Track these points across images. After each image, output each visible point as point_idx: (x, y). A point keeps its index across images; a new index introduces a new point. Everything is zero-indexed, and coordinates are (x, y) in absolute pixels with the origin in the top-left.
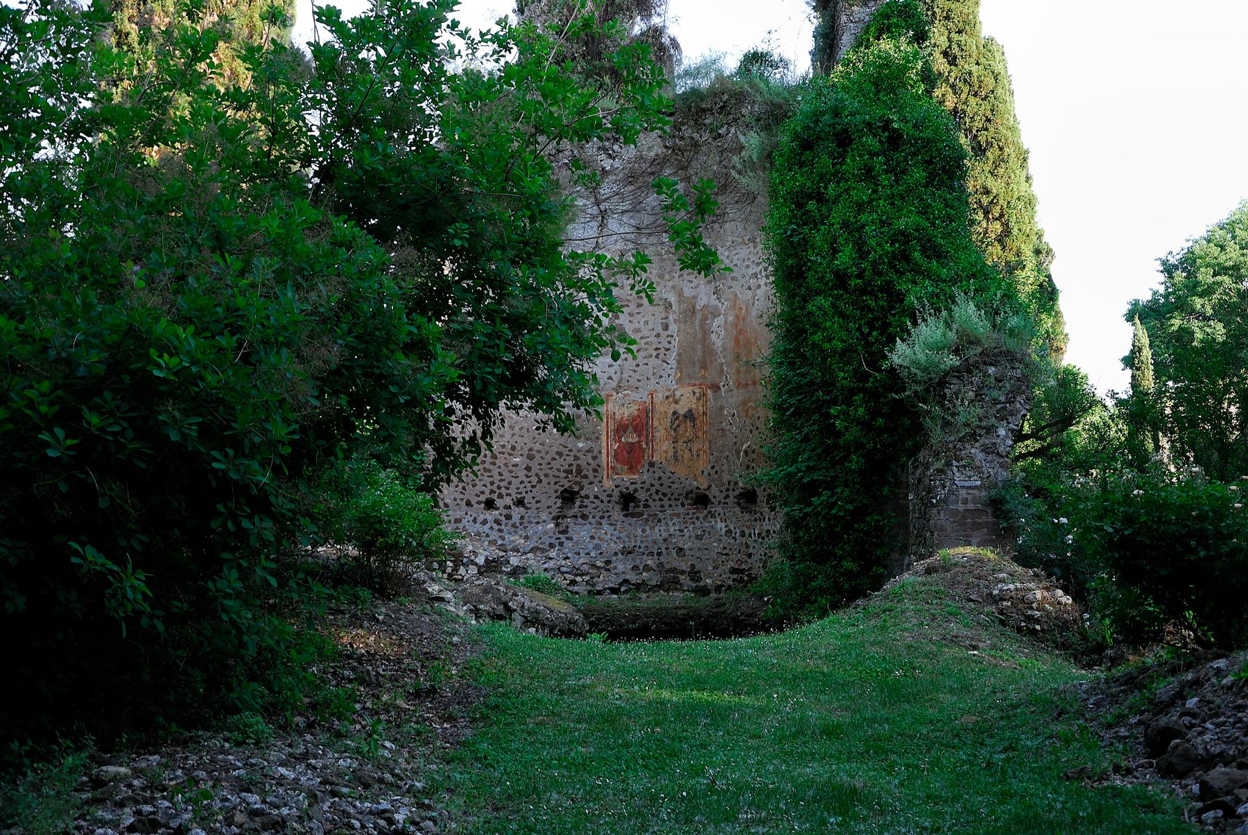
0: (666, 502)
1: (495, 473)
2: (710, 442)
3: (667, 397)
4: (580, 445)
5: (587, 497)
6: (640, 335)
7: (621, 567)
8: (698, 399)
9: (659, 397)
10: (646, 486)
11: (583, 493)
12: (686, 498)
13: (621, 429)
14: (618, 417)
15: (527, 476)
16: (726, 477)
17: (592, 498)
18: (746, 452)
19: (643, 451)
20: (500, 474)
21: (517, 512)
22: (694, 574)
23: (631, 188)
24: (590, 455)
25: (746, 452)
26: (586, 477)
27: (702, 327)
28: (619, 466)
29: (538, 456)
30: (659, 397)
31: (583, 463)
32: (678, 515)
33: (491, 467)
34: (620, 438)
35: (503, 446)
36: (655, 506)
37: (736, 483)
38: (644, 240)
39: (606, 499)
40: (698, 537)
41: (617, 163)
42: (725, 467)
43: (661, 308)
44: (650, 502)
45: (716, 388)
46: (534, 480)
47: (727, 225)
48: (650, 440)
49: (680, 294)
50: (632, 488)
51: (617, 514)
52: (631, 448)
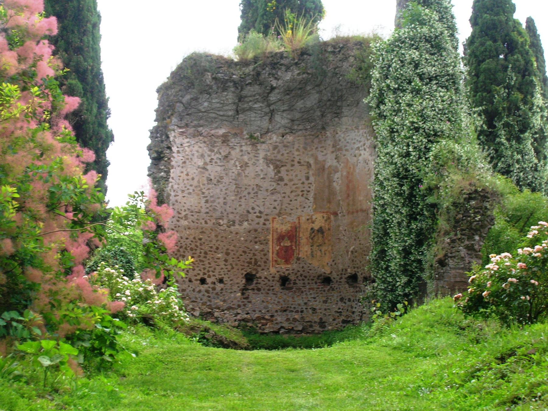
0: (306, 281)
1: (206, 262)
2: (332, 246)
3: (308, 220)
4: (257, 247)
5: (260, 278)
6: (293, 183)
7: (279, 319)
8: (326, 221)
9: (303, 219)
10: (295, 271)
11: (258, 275)
13: (281, 238)
14: (279, 231)
15: (226, 265)
16: (341, 267)
17: (263, 279)
18: (352, 252)
19: (293, 251)
20: (209, 263)
21: (219, 286)
23: (288, 97)
24: (262, 253)
25: (352, 252)
26: (260, 266)
27: (329, 178)
28: (279, 260)
29: (232, 253)
30: (303, 219)
31: (258, 258)
32: (313, 289)
33: (204, 259)
35: (211, 247)
36: (300, 283)
37: (346, 270)
38: (296, 127)
39: (271, 279)
41: (280, 82)
43: (305, 167)
44: (297, 282)
45: (335, 214)
46: (229, 267)
47: (344, 119)
48: (298, 244)
49: (316, 159)
50: (287, 273)
51: (277, 287)
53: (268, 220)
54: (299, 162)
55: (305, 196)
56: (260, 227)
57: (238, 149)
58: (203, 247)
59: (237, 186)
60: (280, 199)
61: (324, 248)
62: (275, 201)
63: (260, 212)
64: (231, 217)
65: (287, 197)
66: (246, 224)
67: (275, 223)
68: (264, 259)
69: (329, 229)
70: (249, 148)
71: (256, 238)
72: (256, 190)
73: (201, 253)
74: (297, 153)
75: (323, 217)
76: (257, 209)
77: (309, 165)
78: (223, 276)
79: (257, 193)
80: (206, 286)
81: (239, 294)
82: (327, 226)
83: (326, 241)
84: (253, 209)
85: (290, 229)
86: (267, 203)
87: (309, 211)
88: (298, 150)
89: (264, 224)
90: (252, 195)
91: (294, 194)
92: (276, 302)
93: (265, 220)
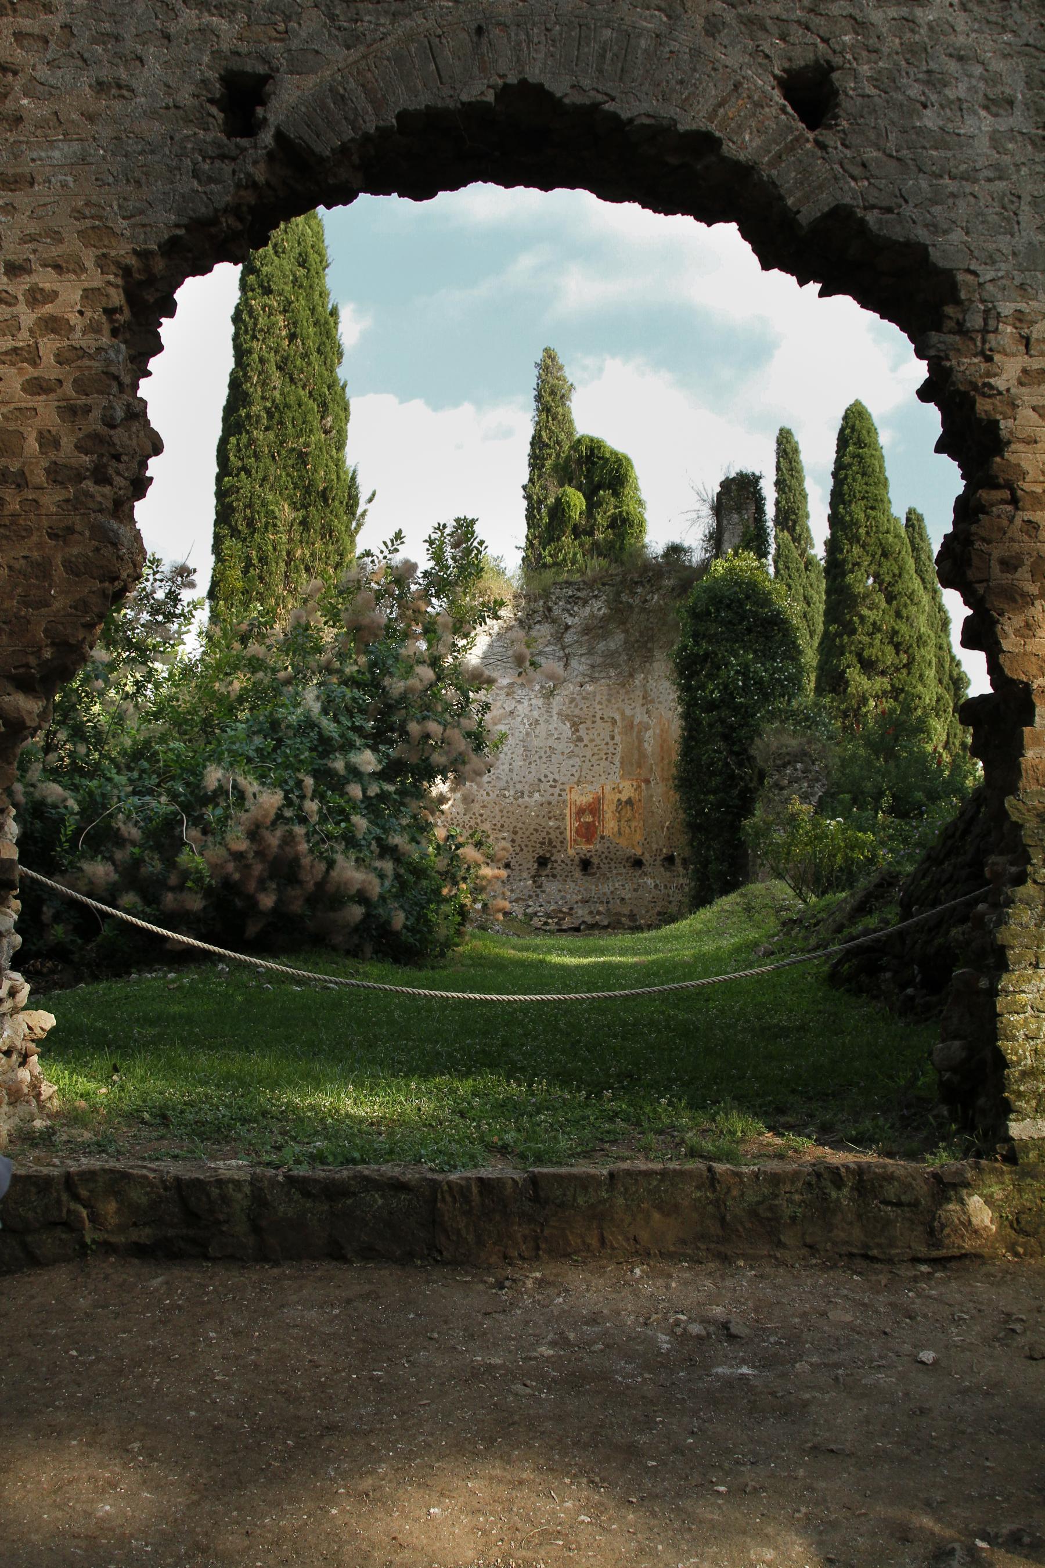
0: (613, 865)
7: (580, 912)
9: (608, 788)
13: (580, 812)
16: (654, 846)
22: (632, 917)
27: (638, 737)
30: (608, 788)
31: (553, 836)
40: (635, 890)
45: (647, 782)
46: (518, 849)
47: (655, 664)
48: (601, 820)
49: (623, 714)
51: (578, 874)
56: (554, 800)
57: (526, 703)
59: (526, 749)
61: (633, 824)
63: (555, 781)
64: (519, 787)
66: (537, 795)
68: (561, 838)
70: (540, 702)
74: (599, 707)
76: (551, 777)
77: (614, 722)
84: (546, 776)
87: (615, 778)
88: (600, 703)
90: (544, 760)
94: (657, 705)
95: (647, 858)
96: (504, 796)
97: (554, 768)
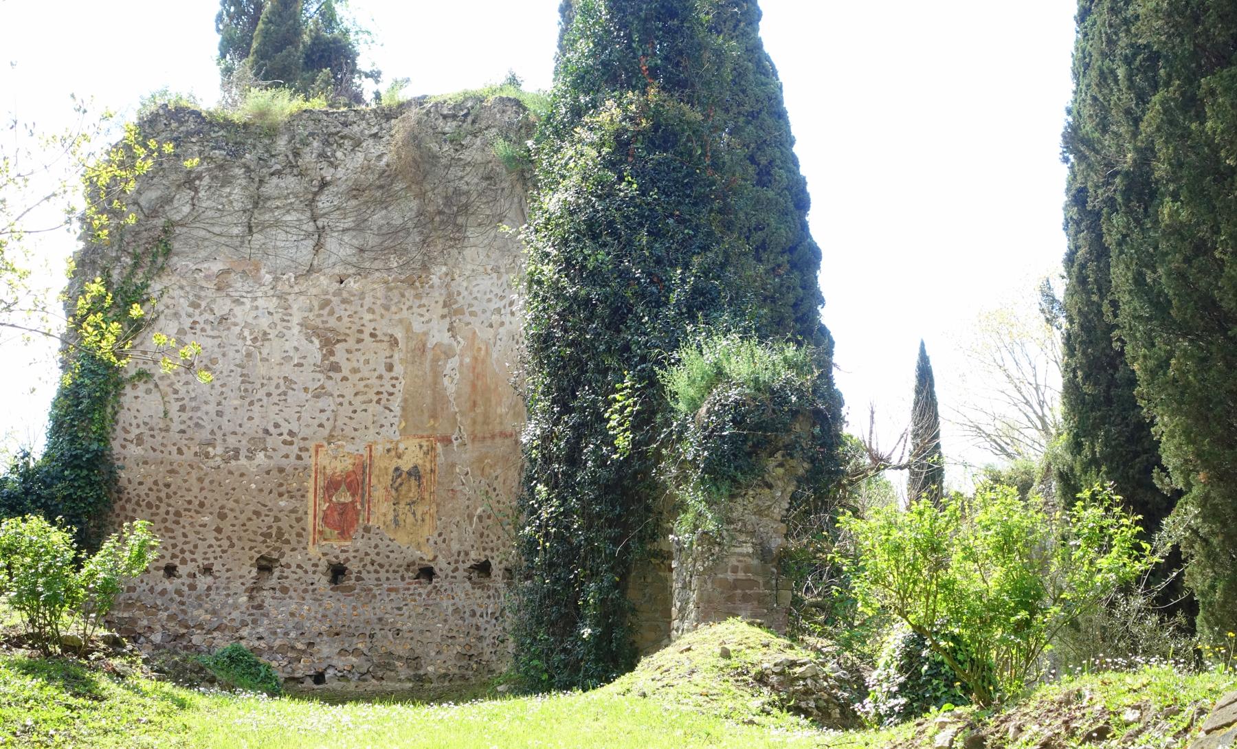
0: (383, 575)
1: (179, 532)
2: (438, 505)
3: (389, 451)
4: (282, 504)
5: (288, 566)
6: (358, 376)
8: (426, 454)
10: (361, 554)
11: (283, 561)
12: (407, 570)
13: (332, 486)
15: (217, 539)
16: (455, 547)
17: (294, 568)
18: (480, 518)
19: (357, 513)
20: (185, 535)
21: (203, 582)
22: (414, 660)
23: (354, 202)
24: (293, 516)
25: (480, 518)
28: (327, 530)
29: (231, 515)
30: (379, 450)
31: (284, 524)
32: (396, 590)
33: (174, 526)
34: (331, 496)
35: (190, 502)
36: (369, 579)
37: (467, 554)
38: (367, 265)
39: (310, 569)
42: (455, 535)
43: (385, 345)
44: (364, 574)
45: (447, 441)
46: (226, 543)
47: (468, 252)
48: (367, 501)
49: (408, 329)
50: (342, 557)
52: (344, 509)
53: (307, 450)
54: (372, 335)
55: (382, 402)
58: (172, 501)
59: (245, 378)
60: (333, 407)
61: (420, 510)
62: (322, 411)
63: (291, 433)
64: (232, 441)
65: (346, 404)
67: (321, 454)
69: (432, 471)
71: (281, 485)
72: (283, 388)
73: (167, 513)
74: (368, 316)
75: (421, 447)
77: (394, 342)
78: (212, 560)
79: (285, 394)
80: (177, 581)
81: (245, 599)
82: (428, 465)
83: (426, 495)
84: (277, 426)
85: (350, 468)
86: (306, 416)
87: (392, 433)
89: (299, 458)
91: (360, 398)
92: (319, 616)
93: (300, 449)
94: (467, 318)
95: (441, 565)
96: (207, 455)
97: (290, 413)
